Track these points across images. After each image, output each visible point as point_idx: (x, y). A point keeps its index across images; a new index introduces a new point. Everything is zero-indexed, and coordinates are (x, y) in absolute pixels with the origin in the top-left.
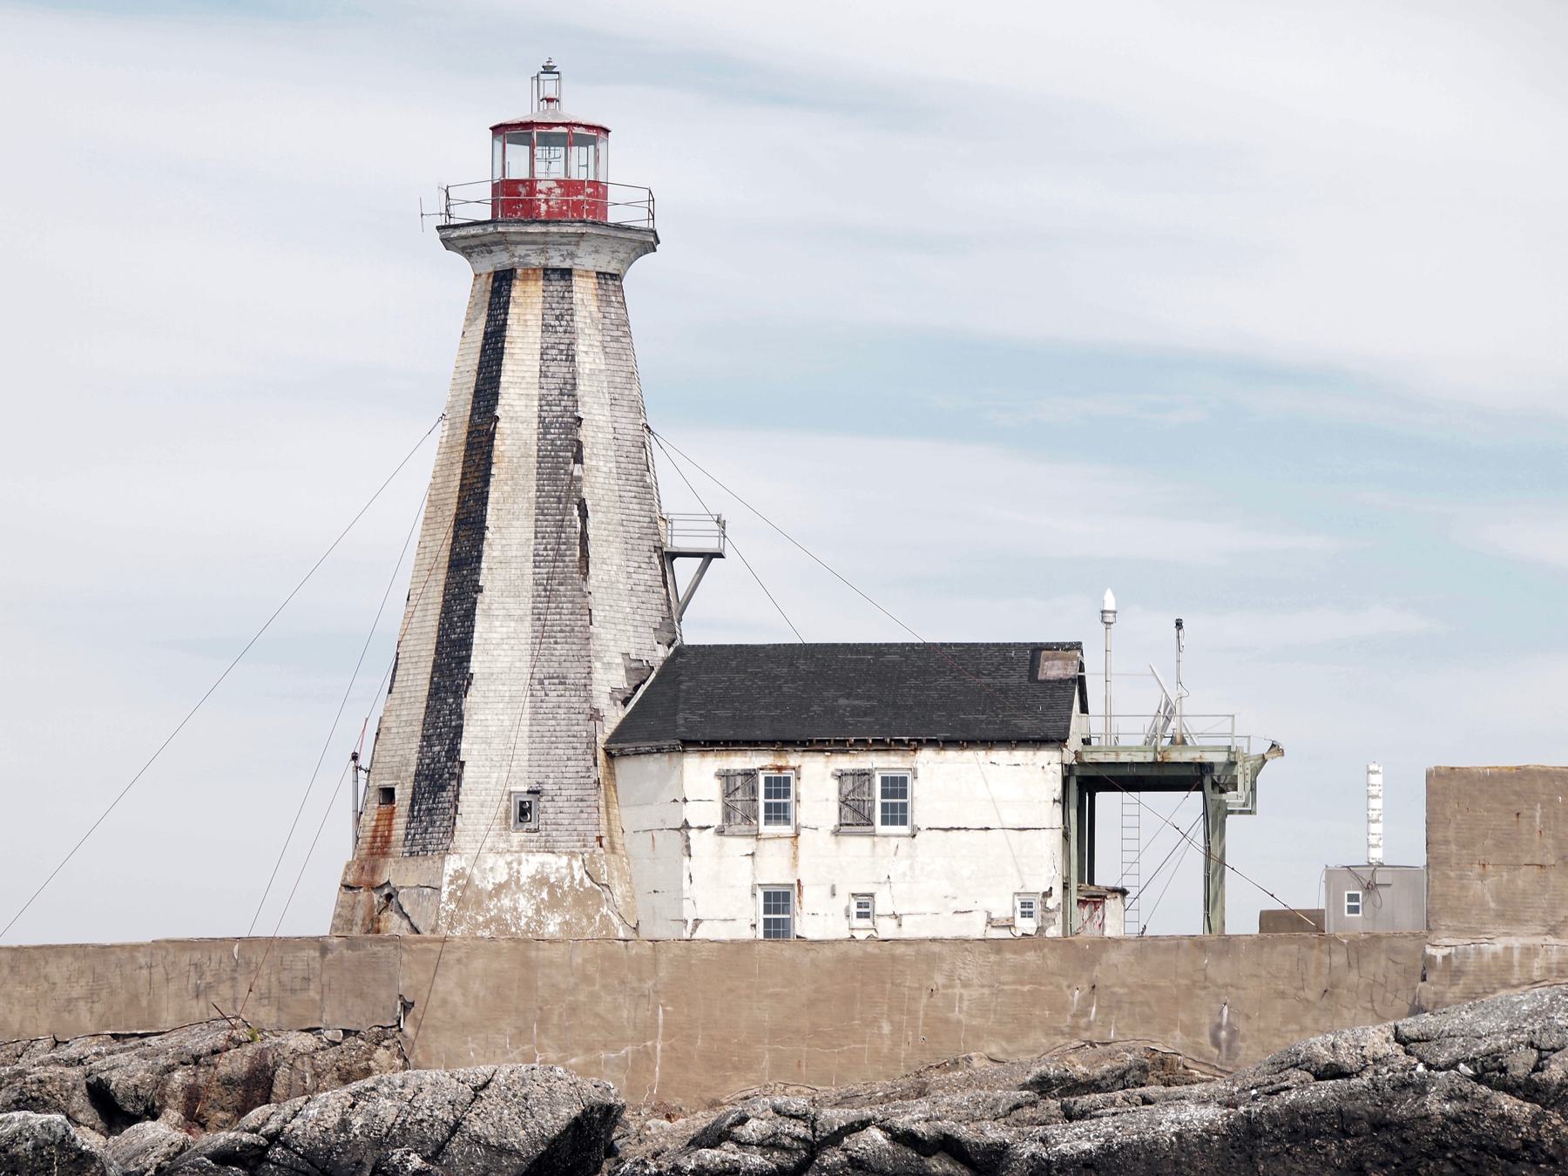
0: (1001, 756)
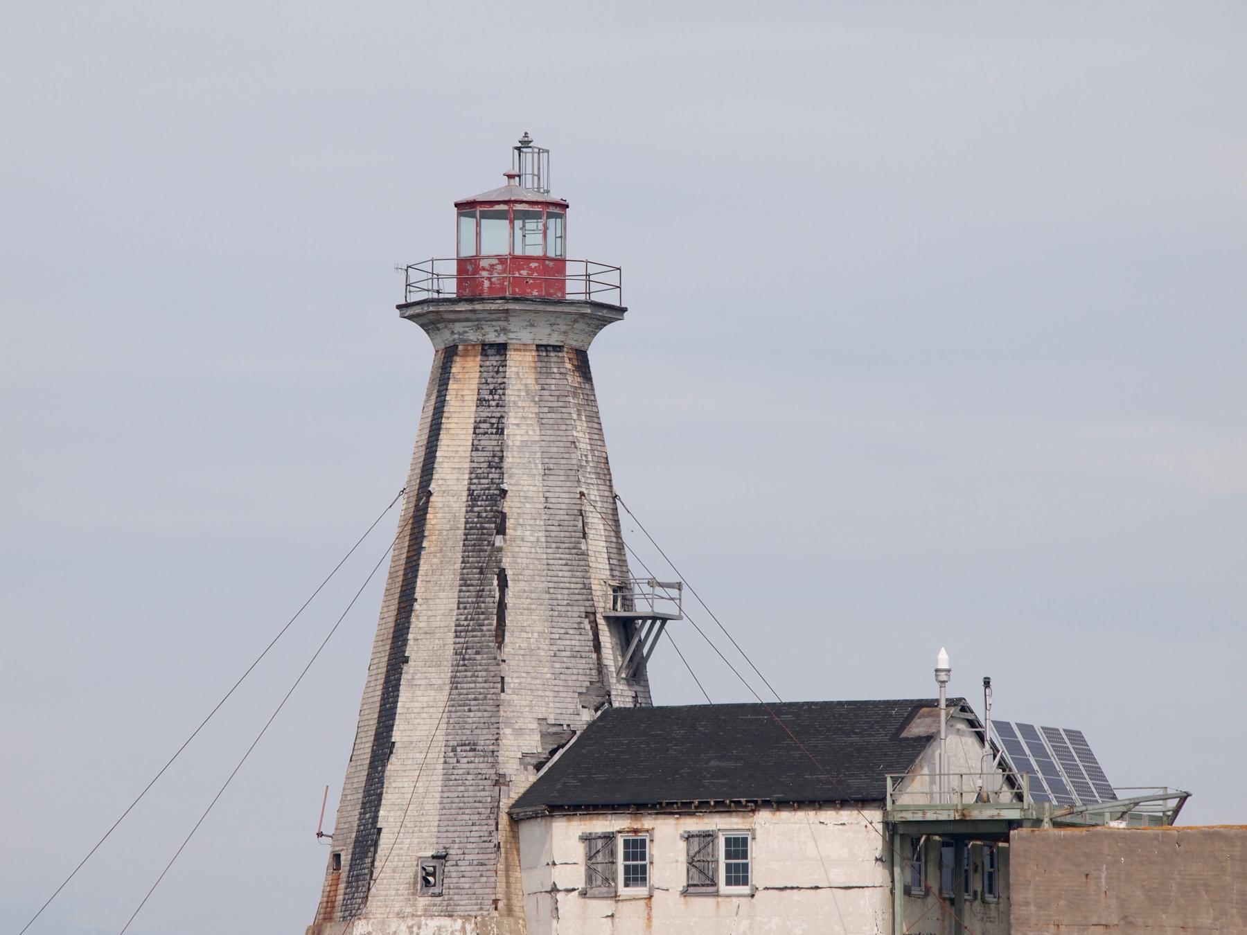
0: (829, 815)
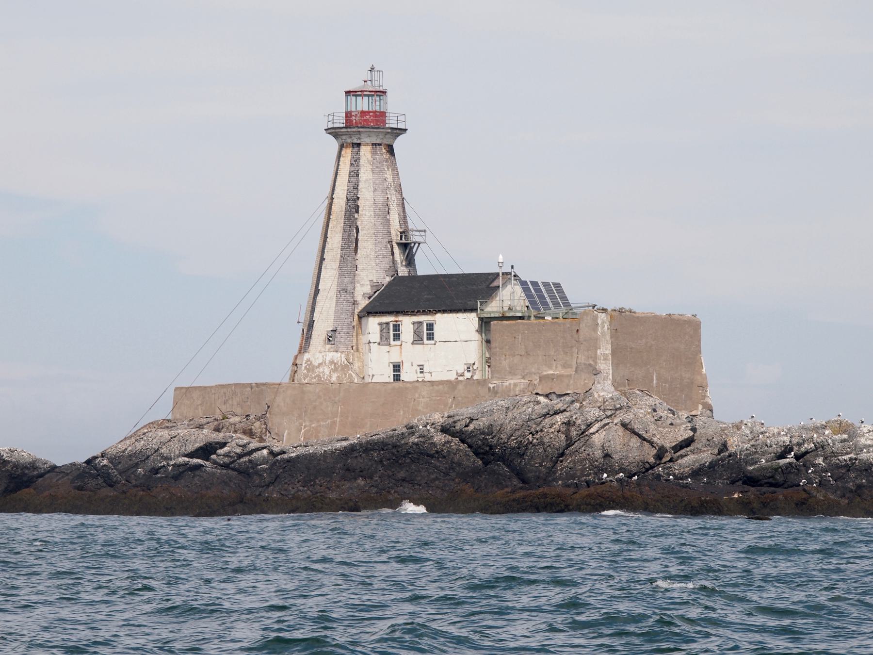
0: (460, 315)
